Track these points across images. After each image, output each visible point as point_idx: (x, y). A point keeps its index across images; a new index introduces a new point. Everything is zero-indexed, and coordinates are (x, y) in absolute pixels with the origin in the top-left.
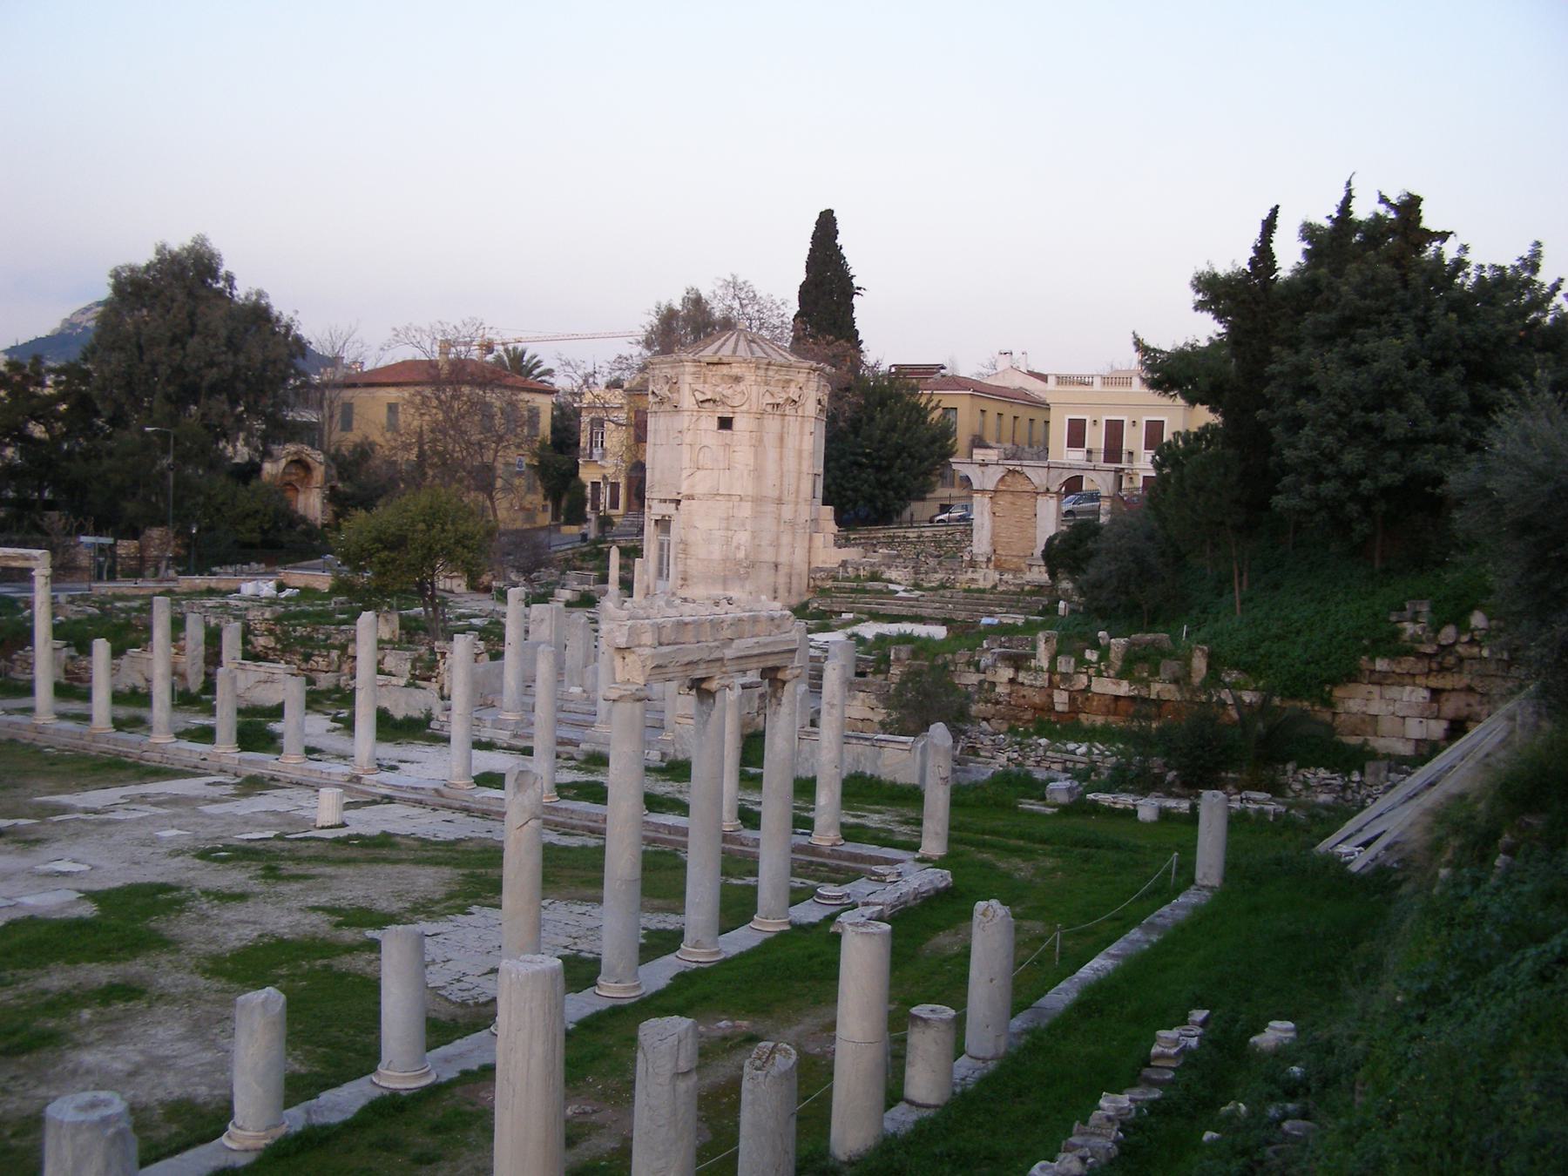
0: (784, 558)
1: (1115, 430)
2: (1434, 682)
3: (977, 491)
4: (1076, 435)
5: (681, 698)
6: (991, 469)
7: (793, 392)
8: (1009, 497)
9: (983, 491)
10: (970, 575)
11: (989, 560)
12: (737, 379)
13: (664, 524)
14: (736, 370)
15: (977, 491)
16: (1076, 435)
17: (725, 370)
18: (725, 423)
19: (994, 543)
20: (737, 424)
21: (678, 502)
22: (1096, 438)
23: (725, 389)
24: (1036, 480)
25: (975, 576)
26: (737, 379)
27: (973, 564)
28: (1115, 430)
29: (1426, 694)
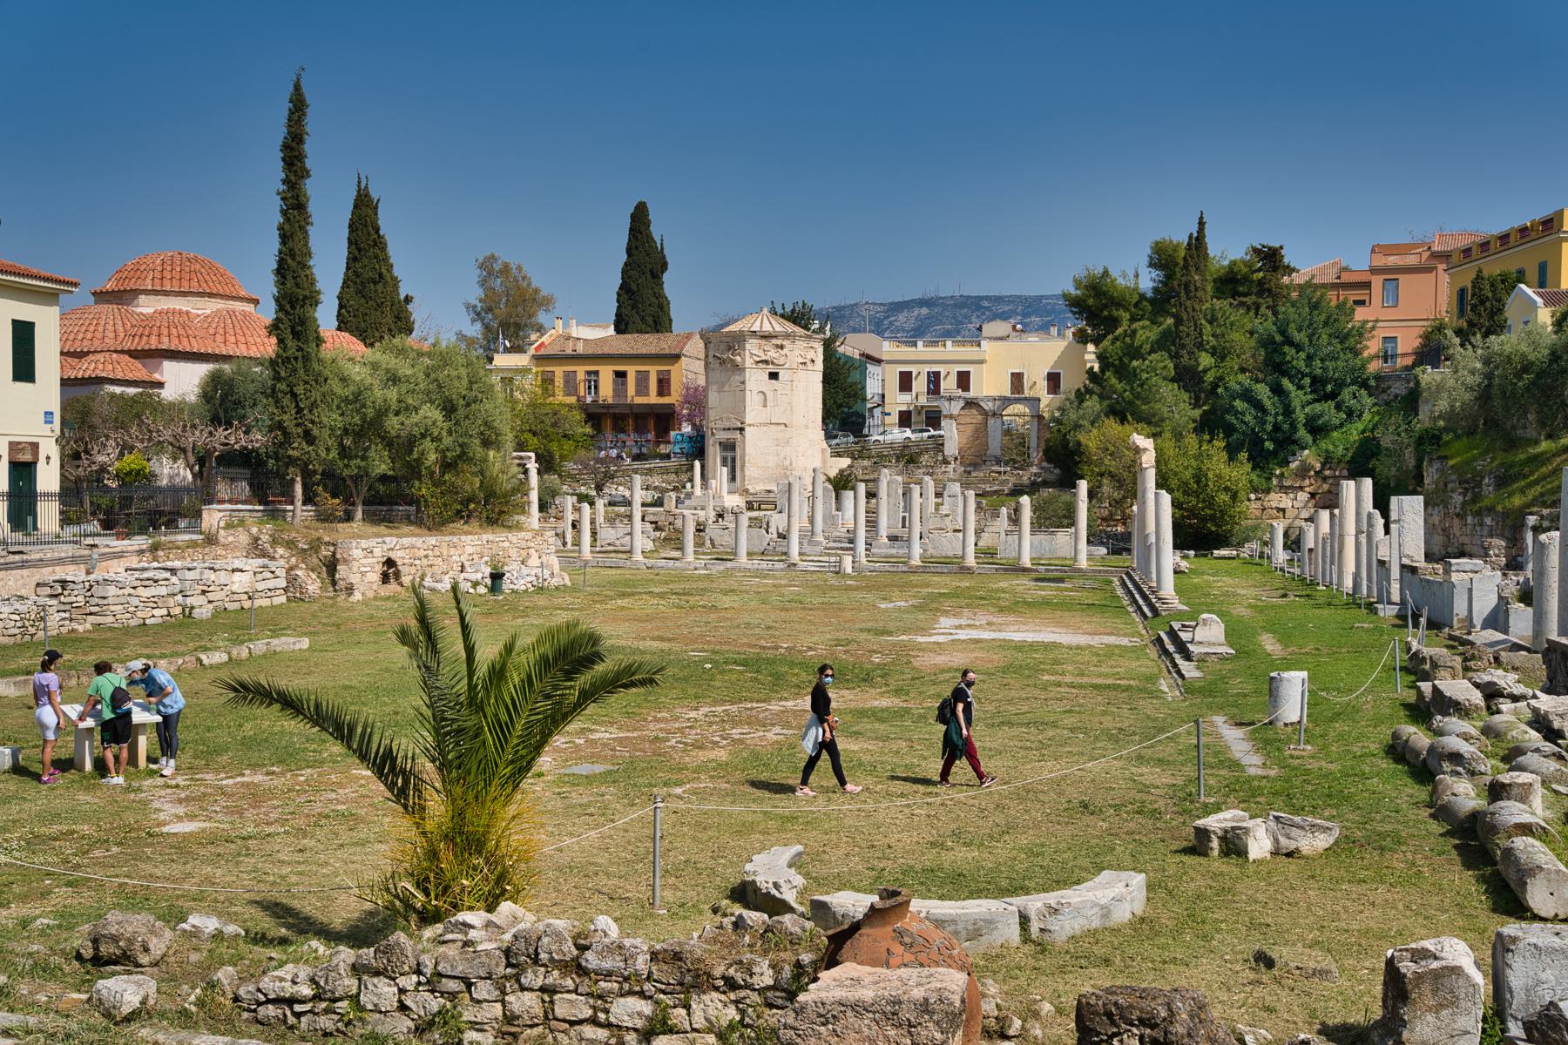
1: (934, 380)
4: (906, 382)
7: (811, 354)
9: (951, 417)
12: (782, 347)
13: (729, 446)
14: (779, 342)
16: (906, 382)
17: (774, 341)
18: (774, 376)
21: (742, 430)
22: (920, 385)
23: (772, 354)
26: (782, 347)
27: (946, 462)
28: (934, 380)
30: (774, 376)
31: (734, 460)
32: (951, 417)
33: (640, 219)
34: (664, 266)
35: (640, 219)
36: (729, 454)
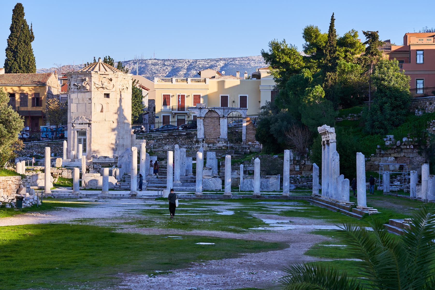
0: (125, 144)
2: (396, 155)
3: (198, 117)
5: (204, 171)
6: (203, 111)
8: (210, 119)
9: (200, 117)
10: (197, 145)
11: (203, 140)
15: (198, 117)
18: (107, 95)
19: (205, 135)
20: (110, 95)
24: (220, 113)
25: (199, 146)
29: (394, 158)
30: (107, 95)
31: (85, 140)
32: (200, 117)
33: (18, 11)
34: (32, 38)
35: (18, 11)
36: (82, 137)
